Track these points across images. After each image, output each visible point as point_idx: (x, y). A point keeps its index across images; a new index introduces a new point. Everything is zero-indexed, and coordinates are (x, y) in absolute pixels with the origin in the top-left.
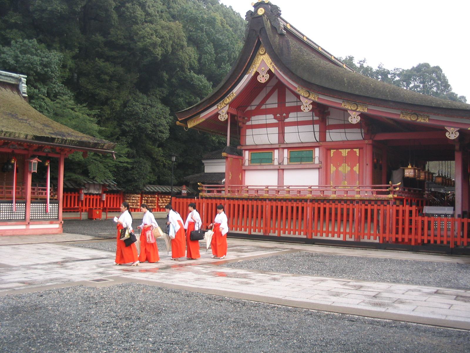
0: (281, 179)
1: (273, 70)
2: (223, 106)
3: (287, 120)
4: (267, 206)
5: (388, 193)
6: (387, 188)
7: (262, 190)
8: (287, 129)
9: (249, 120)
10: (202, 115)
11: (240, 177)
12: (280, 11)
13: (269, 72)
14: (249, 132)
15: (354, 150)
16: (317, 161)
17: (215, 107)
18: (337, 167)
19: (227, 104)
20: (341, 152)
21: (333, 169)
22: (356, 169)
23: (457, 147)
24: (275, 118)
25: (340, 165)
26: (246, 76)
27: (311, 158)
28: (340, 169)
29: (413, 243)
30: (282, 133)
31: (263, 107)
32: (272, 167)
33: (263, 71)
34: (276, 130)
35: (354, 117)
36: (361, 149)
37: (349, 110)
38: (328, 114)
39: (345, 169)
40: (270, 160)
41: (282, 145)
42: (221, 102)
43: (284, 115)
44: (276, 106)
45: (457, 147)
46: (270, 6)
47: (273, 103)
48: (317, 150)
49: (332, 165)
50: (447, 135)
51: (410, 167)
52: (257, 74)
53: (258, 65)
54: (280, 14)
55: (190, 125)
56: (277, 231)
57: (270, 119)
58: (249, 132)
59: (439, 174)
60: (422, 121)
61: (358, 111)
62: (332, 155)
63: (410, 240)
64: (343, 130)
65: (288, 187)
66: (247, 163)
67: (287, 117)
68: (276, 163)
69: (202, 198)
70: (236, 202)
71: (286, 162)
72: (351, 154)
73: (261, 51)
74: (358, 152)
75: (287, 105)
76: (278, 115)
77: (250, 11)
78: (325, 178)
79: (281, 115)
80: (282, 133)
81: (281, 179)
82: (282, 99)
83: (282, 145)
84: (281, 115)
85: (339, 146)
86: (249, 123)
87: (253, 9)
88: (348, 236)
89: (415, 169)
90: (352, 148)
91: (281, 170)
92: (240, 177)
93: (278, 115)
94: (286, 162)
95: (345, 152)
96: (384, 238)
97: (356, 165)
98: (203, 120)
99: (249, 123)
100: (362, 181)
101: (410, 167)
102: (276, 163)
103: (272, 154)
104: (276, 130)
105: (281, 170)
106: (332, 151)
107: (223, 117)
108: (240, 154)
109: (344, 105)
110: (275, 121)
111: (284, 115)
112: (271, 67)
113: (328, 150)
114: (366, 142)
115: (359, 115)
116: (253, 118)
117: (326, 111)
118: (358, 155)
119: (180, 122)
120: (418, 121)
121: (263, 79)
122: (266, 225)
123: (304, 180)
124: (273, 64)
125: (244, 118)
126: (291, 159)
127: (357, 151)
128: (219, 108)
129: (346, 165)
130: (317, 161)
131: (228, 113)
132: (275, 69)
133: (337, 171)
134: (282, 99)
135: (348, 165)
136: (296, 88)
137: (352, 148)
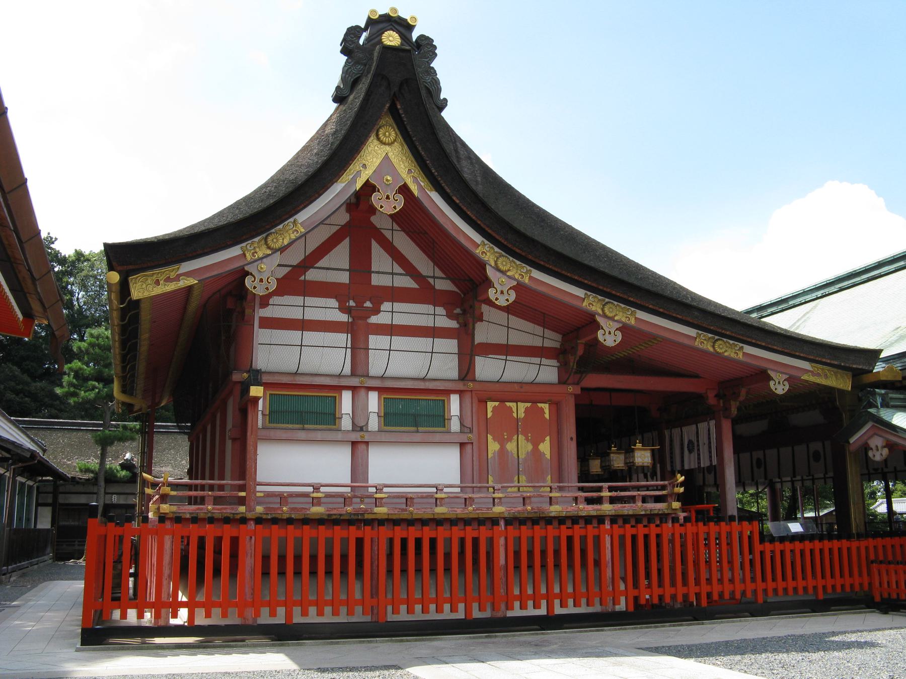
0: (359, 469)
1: (414, 188)
3: (374, 319)
4: (377, 543)
6: (663, 488)
7: (306, 495)
8: (375, 341)
13: (404, 190)
16: (455, 425)
17: (235, 251)
18: (502, 443)
19: (275, 251)
20: (510, 408)
21: (493, 447)
22: (545, 447)
24: (343, 309)
25: (510, 439)
27: (440, 419)
28: (511, 446)
30: (359, 351)
31: (312, 275)
32: (339, 436)
35: (610, 333)
36: (556, 406)
37: (599, 315)
39: (520, 447)
41: (359, 379)
43: (368, 304)
47: (336, 267)
51: (639, 445)
52: (369, 188)
56: (461, 606)
57: (326, 309)
58: (262, 335)
60: (733, 355)
61: (617, 321)
62: (489, 415)
64: (537, 360)
65: (379, 489)
67: (376, 311)
68: (346, 423)
71: (374, 424)
74: (547, 411)
76: (352, 303)
79: (360, 304)
80: (359, 351)
81: (359, 469)
84: (360, 304)
88: (297, 610)
90: (534, 402)
95: (520, 409)
96: (636, 599)
97: (543, 441)
100: (560, 477)
101: (639, 445)
106: (491, 405)
109: (590, 304)
113: (483, 402)
114: (570, 389)
118: (547, 416)
120: (726, 354)
122: (375, 592)
123: (420, 470)
124: (417, 172)
126: (389, 418)
127: (546, 407)
128: (249, 256)
130: (455, 425)
133: (502, 452)
136: (477, 246)
137: (534, 402)
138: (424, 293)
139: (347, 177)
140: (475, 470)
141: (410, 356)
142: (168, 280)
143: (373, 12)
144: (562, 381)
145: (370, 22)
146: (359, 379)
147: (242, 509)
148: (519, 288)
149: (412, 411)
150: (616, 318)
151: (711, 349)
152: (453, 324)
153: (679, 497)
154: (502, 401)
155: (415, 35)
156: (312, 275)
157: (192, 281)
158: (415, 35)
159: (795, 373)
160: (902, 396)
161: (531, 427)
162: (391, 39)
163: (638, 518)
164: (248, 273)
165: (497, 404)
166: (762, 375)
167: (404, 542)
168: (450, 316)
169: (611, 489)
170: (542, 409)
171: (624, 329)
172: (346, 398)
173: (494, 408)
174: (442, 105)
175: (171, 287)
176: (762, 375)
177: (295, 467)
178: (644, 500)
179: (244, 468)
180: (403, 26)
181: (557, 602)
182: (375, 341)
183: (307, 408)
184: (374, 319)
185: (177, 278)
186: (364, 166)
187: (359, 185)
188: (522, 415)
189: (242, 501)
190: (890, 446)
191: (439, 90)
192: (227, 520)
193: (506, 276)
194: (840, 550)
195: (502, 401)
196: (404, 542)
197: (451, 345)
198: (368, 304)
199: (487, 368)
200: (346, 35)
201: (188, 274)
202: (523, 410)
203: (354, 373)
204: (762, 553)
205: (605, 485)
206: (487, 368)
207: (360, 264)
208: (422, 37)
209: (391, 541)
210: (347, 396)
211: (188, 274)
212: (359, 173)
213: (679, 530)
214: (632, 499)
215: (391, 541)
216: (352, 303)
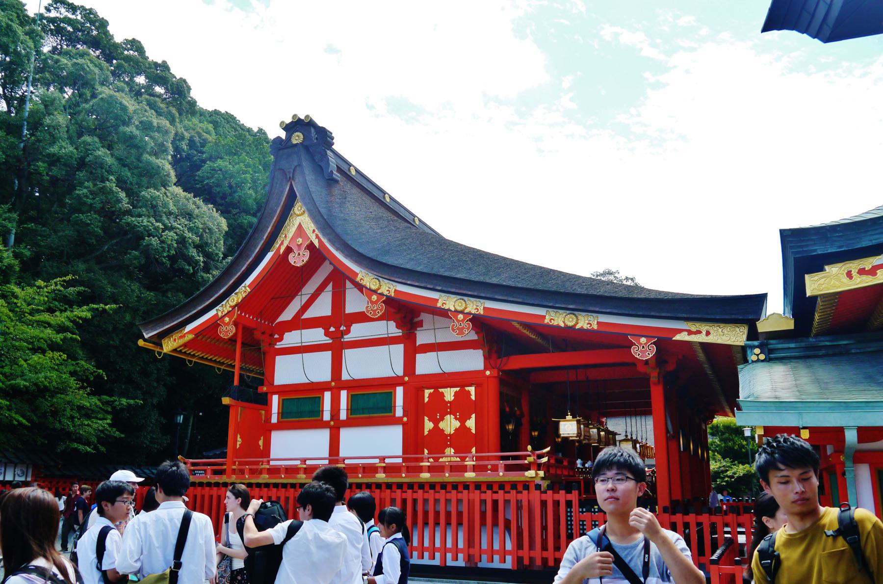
2: (226, 312)
5: (527, 468)
9: (281, 339)
10: (190, 327)
11: (261, 443)
12: (333, 138)
14: (280, 360)
15: (467, 388)
16: (399, 412)
18: (436, 422)
20: (442, 393)
22: (471, 423)
23: (654, 378)
24: (327, 334)
25: (442, 419)
26: (270, 255)
28: (442, 425)
33: (299, 246)
34: (329, 354)
36: (478, 387)
38: (420, 324)
39: (450, 424)
42: (224, 303)
43: (343, 328)
45: (654, 378)
46: (313, 130)
48: (400, 391)
49: (426, 418)
50: (633, 350)
51: (569, 417)
52: (289, 250)
53: (290, 235)
54: (333, 144)
55: (169, 346)
57: (317, 335)
58: (280, 360)
59: (626, 436)
60: (586, 327)
62: (426, 400)
66: (274, 419)
67: (348, 332)
68: (327, 416)
71: (343, 416)
72: (462, 396)
73: (298, 208)
77: (279, 137)
78: (413, 442)
79: (338, 328)
82: (338, 301)
84: (338, 328)
86: (279, 345)
87: (283, 135)
89: (578, 422)
90: (462, 386)
92: (261, 443)
93: (332, 329)
94: (343, 416)
95: (449, 394)
98: (191, 336)
99: (279, 345)
101: (569, 417)
102: (327, 416)
103: (319, 401)
104: (329, 354)
105: (335, 427)
106: (427, 392)
107: (227, 331)
108: (264, 401)
111: (343, 328)
112: (314, 237)
114: (488, 373)
115: (470, 320)
116: (287, 335)
117: (416, 320)
118: (473, 397)
119: (145, 340)
120: (577, 327)
125: (272, 335)
127: (472, 389)
128: (220, 314)
129: (452, 417)
130: (399, 412)
131: (236, 324)
132: (320, 241)
134: (338, 301)
135: (456, 419)
137: (462, 386)
142: (181, 337)
144: (486, 369)
147: (224, 477)
149: (370, 403)
150: (466, 311)
151: (562, 325)
152: (398, 333)
154: (436, 388)
156: (307, 315)
160: (792, 345)
161: (461, 408)
163: (502, 485)
164: (220, 325)
165: (432, 391)
166: (619, 342)
170: (469, 392)
172: (327, 395)
173: (430, 394)
183: (303, 407)
184: (347, 338)
185: (184, 336)
195: (436, 388)
197: (398, 350)
202: (453, 394)
203: (333, 380)
206: (426, 364)
210: (327, 395)
211: (189, 332)
212: (282, 243)
216: (332, 329)
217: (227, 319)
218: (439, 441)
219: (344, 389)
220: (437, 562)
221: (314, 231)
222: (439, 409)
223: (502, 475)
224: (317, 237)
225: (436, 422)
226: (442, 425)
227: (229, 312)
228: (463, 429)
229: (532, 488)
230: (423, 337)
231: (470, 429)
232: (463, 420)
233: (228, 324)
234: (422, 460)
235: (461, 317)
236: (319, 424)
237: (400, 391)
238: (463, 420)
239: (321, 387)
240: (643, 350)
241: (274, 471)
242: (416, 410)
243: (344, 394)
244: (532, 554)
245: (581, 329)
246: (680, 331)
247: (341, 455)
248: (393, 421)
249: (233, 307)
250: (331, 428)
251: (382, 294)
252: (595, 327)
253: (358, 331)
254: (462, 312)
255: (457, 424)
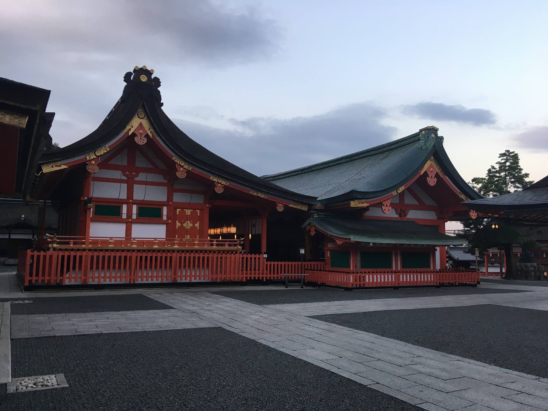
0: (128, 231)
1: (151, 135)
2: (92, 158)
3: (136, 179)
8: (135, 186)
13: (147, 136)
16: (165, 218)
17: (83, 157)
18: (182, 223)
22: (197, 225)
28: (185, 225)
29: (265, 280)
33: (141, 134)
39: (188, 225)
40: (119, 213)
43: (134, 173)
44: (125, 163)
48: (165, 209)
50: (277, 208)
52: (134, 135)
62: (178, 213)
63: (263, 278)
68: (124, 216)
69: (55, 249)
70: (101, 254)
71: (134, 217)
75: (138, 164)
81: (128, 231)
83: (130, 201)
85: (184, 206)
90: (194, 209)
91: (129, 223)
93: (127, 173)
94: (134, 217)
95: (188, 212)
102: (124, 216)
104: (125, 186)
106: (178, 210)
110: (124, 178)
113: (175, 209)
121: (141, 141)
124: (152, 130)
126: (139, 214)
130: (165, 218)
132: (153, 135)
137: (194, 209)
138: (155, 170)
139: (126, 131)
140: (170, 233)
141: (149, 193)
143: (137, 67)
144: (205, 203)
145: (135, 71)
146: (130, 201)
147: (84, 246)
148: (188, 172)
149: (149, 213)
153: (240, 245)
154: (183, 209)
155: (153, 77)
157: (65, 167)
158: (153, 77)
159: (287, 204)
162: (144, 78)
167: (141, 257)
168: (165, 178)
169: (216, 241)
171: (225, 187)
172: (125, 208)
174: (162, 104)
175: (58, 168)
176: (274, 205)
177: (104, 231)
178: (230, 245)
179: (84, 231)
180: (148, 73)
181: (193, 278)
182: (135, 186)
183: (109, 211)
184: (136, 179)
185: (60, 166)
186: (132, 127)
187: (130, 133)
188: (189, 214)
189: (84, 243)
190: (316, 230)
191: (161, 99)
192: (78, 250)
193: (183, 168)
194: (278, 265)
195: (183, 209)
196: (141, 257)
198: (134, 173)
199: (178, 198)
200: (126, 75)
201: (65, 164)
204: (267, 265)
205: (215, 240)
207: (132, 160)
208: (156, 78)
209: (137, 257)
212: (130, 129)
213: (241, 256)
214: (224, 245)
215: (137, 257)
216: (127, 173)
217: (93, 162)
218: (183, 232)
219: (135, 204)
220: (188, 281)
221: (149, 129)
222: (184, 218)
223: (227, 247)
224: (151, 132)
225: (182, 223)
226: (185, 225)
227: (94, 159)
228: (194, 227)
229: (238, 252)
230: (176, 187)
231: (196, 227)
232: (194, 223)
233: (94, 165)
234: (175, 240)
235: (219, 185)
236: (120, 221)
237: (165, 209)
238: (194, 223)
239: (122, 202)
240: (280, 208)
241: (95, 242)
242: (172, 216)
243: (135, 208)
244: (216, 276)
245: (262, 198)
246: (291, 204)
247: (132, 237)
248: (161, 222)
249: (98, 157)
250: (127, 223)
251: (185, 168)
252: (266, 198)
253: (142, 177)
254: (220, 183)
255: (191, 225)
